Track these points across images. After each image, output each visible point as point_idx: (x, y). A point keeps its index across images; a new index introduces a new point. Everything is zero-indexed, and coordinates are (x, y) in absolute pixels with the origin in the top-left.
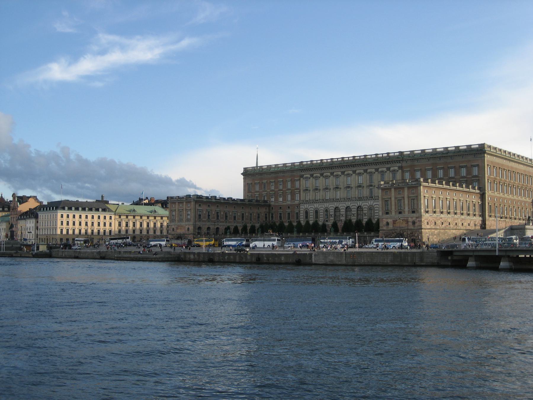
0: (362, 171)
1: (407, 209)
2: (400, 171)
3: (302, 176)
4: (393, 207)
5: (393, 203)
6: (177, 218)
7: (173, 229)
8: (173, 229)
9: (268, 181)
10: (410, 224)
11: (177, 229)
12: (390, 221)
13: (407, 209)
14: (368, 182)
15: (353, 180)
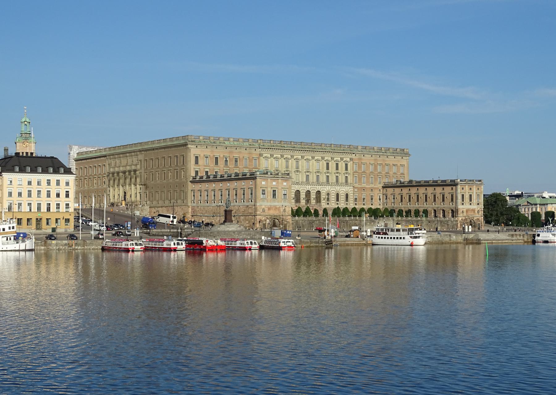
0: (320, 158)
1: (475, 201)
2: (351, 162)
3: (261, 155)
4: (467, 200)
5: (467, 197)
6: (269, 197)
7: (264, 211)
8: (264, 211)
9: (222, 156)
10: (476, 212)
11: (269, 209)
12: (465, 210)
13: (475, 201)
14: (325, 168)
15: (314, 166)
